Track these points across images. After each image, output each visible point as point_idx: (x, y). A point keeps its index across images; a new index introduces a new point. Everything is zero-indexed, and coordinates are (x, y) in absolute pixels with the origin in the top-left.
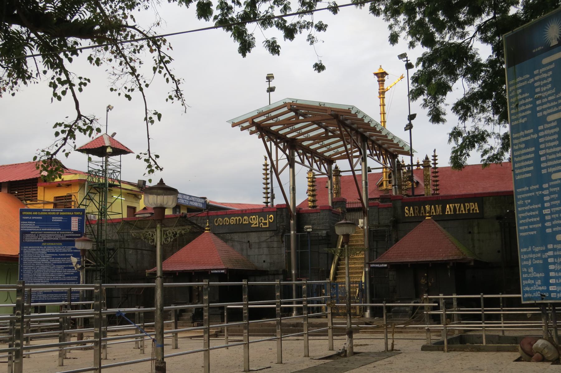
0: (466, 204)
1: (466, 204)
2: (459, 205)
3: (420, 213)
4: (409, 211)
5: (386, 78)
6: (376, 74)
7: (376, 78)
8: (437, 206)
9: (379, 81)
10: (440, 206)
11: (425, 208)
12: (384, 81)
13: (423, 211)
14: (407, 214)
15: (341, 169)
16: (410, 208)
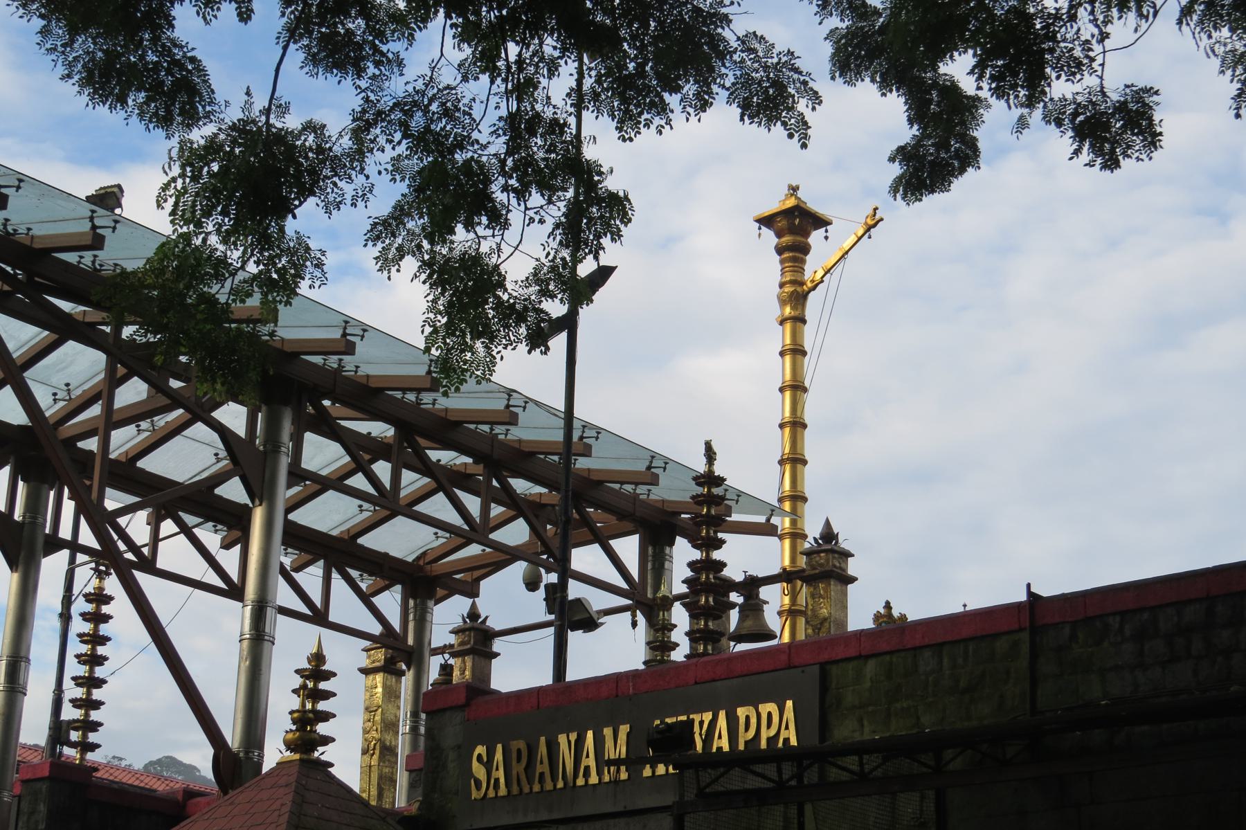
0: (741, 712)
1: (741, 712)
2: (707, 717)
3: (530, 782)
4: (488, 764)
5: (816, 238)
6: (766, 221)
7: (770, 238)
8: (608, 732)
9: (780, 250)
10: (624, 729)
11: (553, 747)
12: (805, 249)
13: (545, 768)
14: (478, 784)
15: (495, 624)
16: (491, 753)
